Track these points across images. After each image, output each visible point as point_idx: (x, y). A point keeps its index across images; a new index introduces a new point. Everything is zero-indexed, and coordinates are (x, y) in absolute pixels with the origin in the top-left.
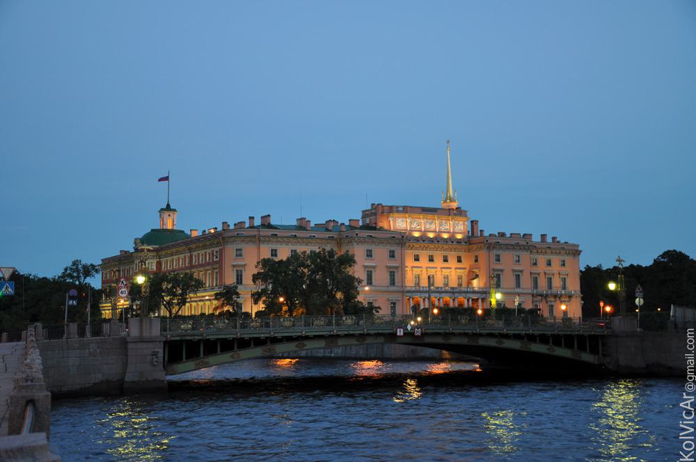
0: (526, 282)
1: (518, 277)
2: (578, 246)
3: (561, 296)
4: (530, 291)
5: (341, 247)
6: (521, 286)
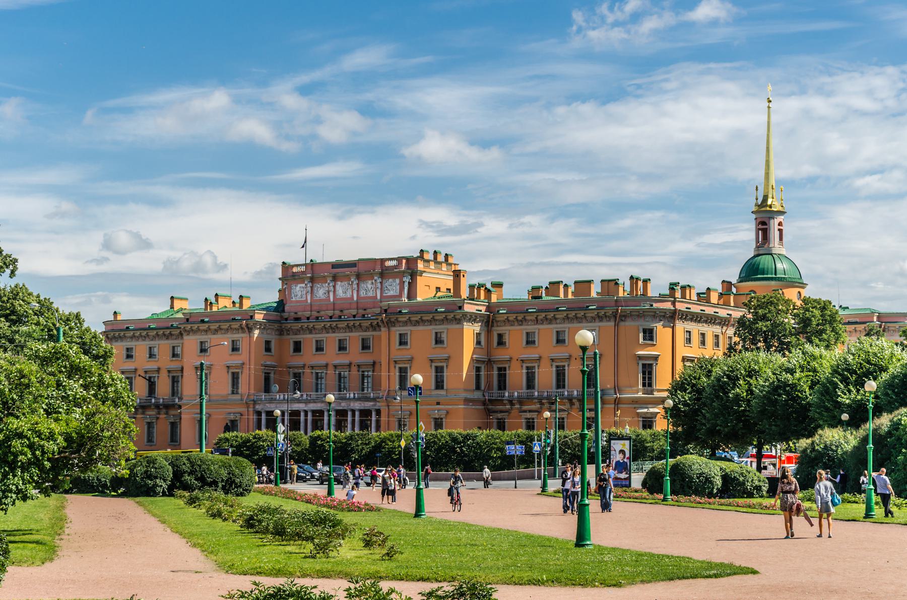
1: (439, 370)
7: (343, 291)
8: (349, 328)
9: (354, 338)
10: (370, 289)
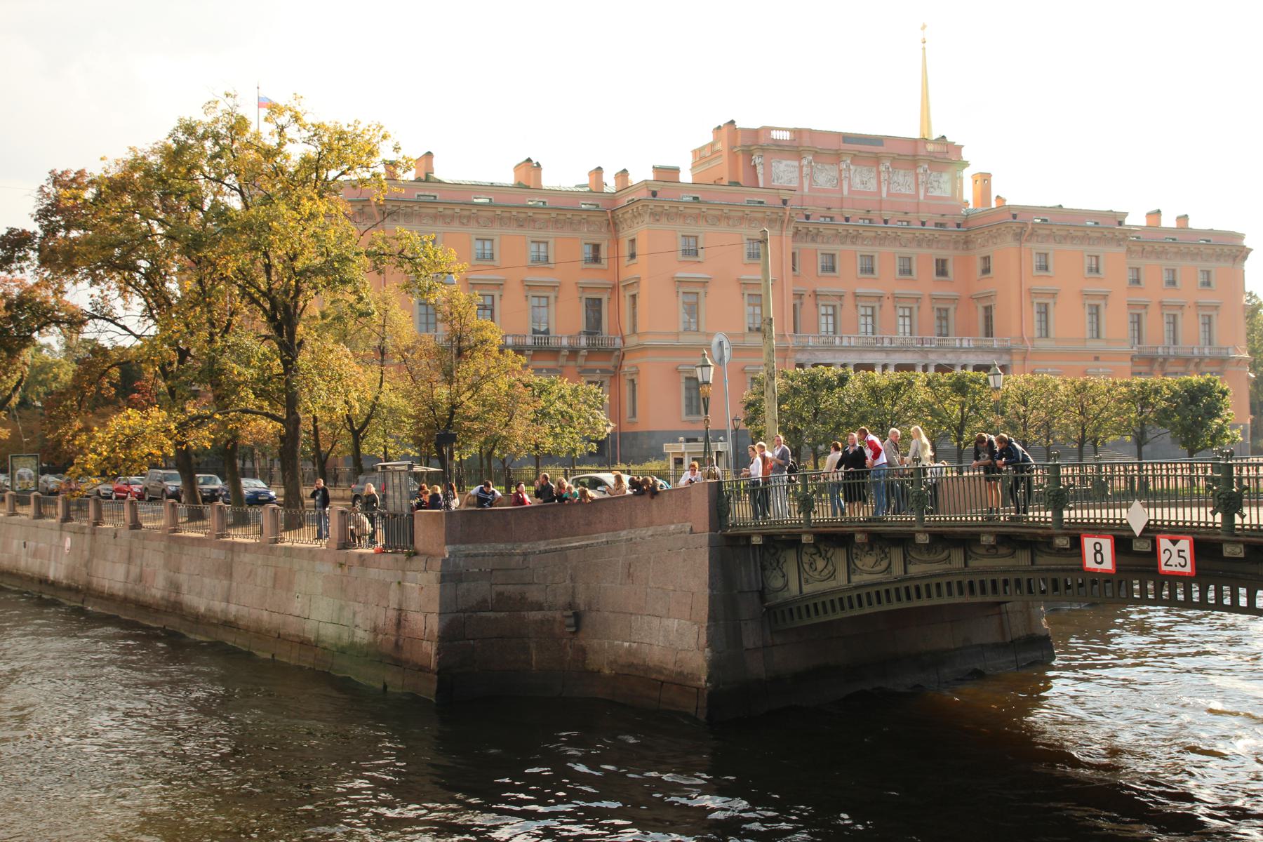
0: (1116, 322)
1: (1095, 311)
2: (1241, 237)
3: (1165, 359)
4: (1126, 348)
5: (617, 231)
6: (1103, 335)
7: (860, 181)
8: (881, 239)
9: (887, 256)
10: (902, 184)
